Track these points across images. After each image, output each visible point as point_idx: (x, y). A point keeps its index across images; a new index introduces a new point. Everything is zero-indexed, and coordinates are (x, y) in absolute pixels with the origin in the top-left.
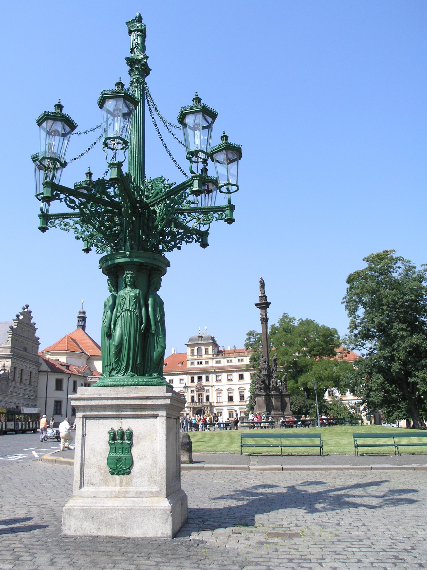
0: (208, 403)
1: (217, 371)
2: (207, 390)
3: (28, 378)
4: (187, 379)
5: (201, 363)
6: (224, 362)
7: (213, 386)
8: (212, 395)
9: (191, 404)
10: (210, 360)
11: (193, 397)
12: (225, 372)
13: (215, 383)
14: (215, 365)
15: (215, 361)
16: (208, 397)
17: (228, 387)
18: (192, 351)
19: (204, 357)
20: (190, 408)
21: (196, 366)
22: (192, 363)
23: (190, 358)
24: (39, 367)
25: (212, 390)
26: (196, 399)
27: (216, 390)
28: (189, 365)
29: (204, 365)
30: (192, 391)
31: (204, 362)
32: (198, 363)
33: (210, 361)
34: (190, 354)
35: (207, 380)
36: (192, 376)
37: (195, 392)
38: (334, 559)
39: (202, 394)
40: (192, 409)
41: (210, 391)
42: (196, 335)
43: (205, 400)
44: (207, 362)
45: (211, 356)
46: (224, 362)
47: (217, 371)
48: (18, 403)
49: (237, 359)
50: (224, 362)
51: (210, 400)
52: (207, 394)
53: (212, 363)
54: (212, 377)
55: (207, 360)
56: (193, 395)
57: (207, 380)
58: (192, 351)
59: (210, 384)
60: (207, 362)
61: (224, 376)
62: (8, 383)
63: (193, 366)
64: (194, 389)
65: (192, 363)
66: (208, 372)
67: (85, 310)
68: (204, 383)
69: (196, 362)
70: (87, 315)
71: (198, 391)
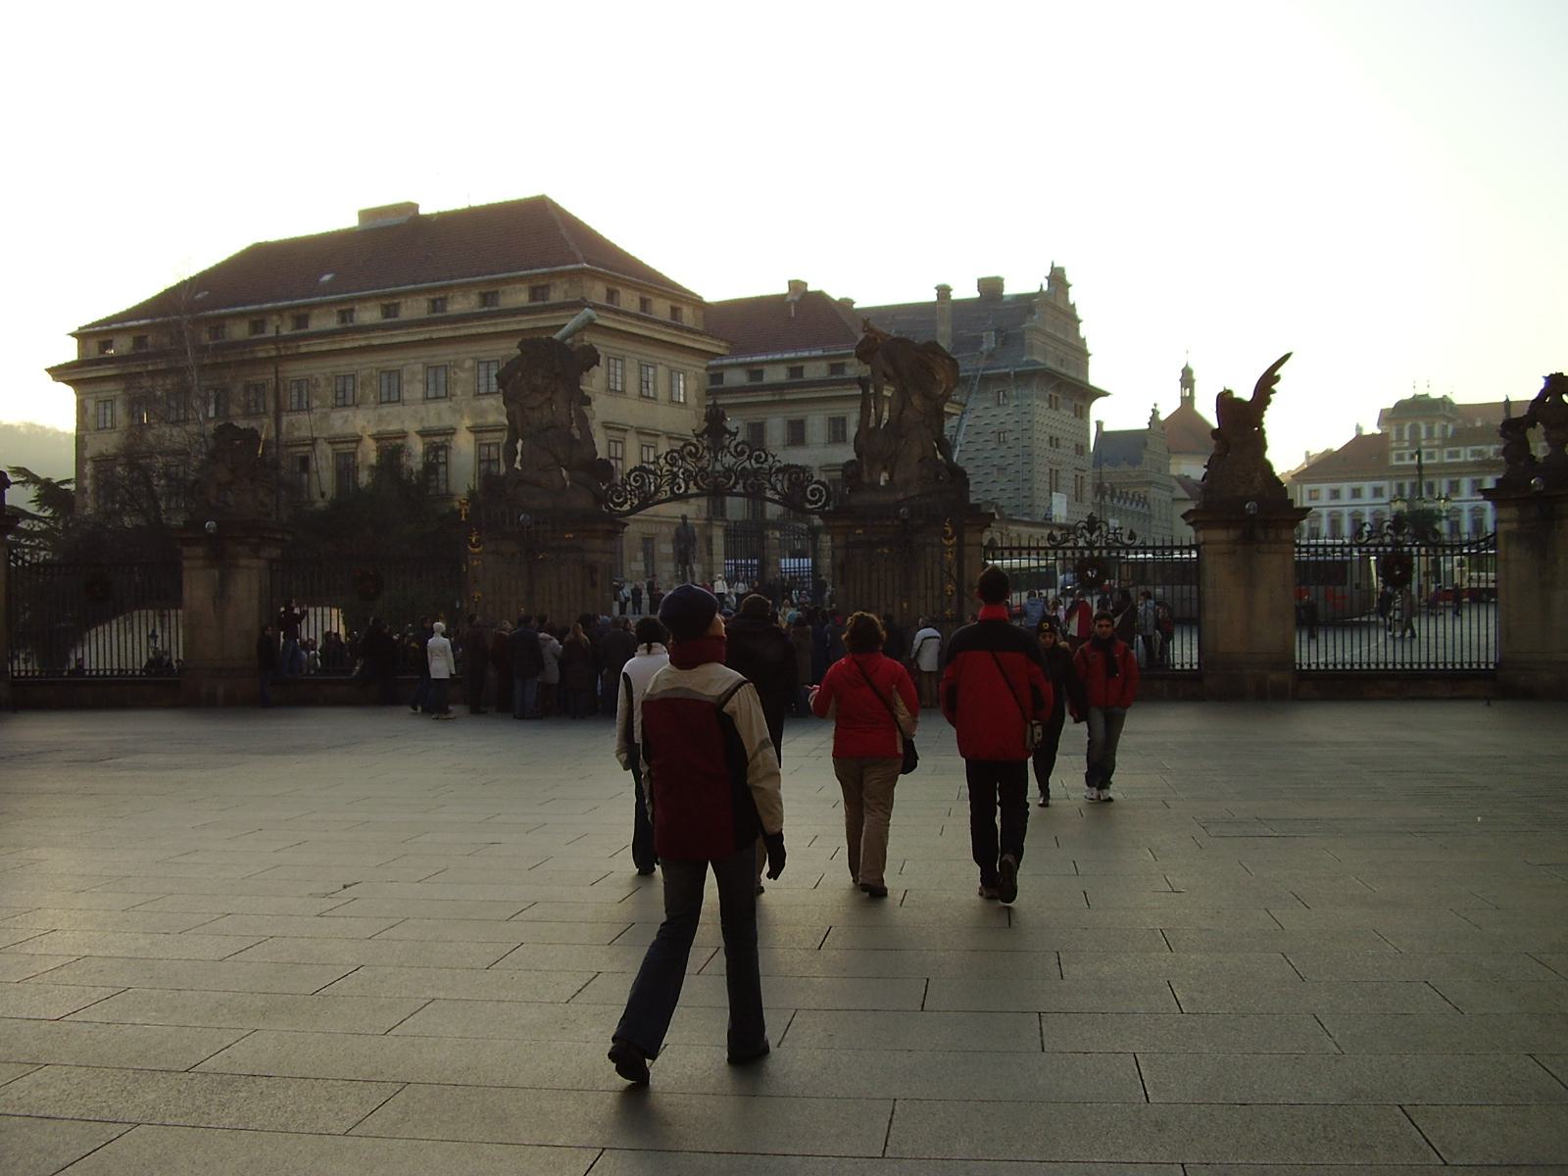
10: (1436, 450)
14: (1447, 460)
15: (1445, 451)
18: (1400, 433)
22: (1400, 457)
23: (1394, 445)
34: (1394, 438)
36: (1400, 481)
45: (1436, 442)
46: (1466, 456)
50: (1466, 456)
53: (1442, 457)
58: (1400, 433)
63: (1400, 463)
65: (1400, 457)
69: (1407, 457)
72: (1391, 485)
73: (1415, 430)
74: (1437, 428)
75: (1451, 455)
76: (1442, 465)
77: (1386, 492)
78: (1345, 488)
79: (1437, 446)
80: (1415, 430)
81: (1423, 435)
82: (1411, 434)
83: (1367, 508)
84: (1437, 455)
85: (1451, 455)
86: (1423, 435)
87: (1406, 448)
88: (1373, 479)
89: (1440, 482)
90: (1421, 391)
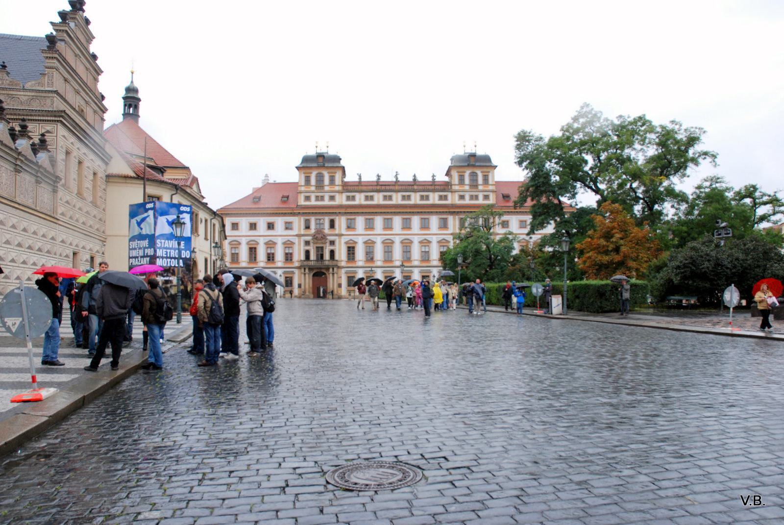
0: (334, 263)
1: (351, 211)
2: (332, 243)
3: (90, 187)
4: (298, 222)
5: (322, 198)
6: (360, 199)
7: (340, 235)
8: (340, 250)
9: (306, 263)
11: (307, 253)
12: (362, 214)
13: (344, 232)
14: (345, 202)
15: (344, 195)
16: (332, 253)
17: (366, 238)
18: (308, 180)
19: (327, 188)
20: (305, 269)
21: (313, 202)
22: (308, 198)
23: (303, 189)
24: (107, 164)
25: (340, 242)
26: (313, 257)
27: (346, 243)
28: (302, 202)
29: (327, 202)
30: (307, 243)
31: (327, 198)
32: (317, 197)
33: (337, 196)
35: (332, 225)
37: (312, 244)
38: (447, 470)
39: (322, 248)
40: (307, 271)
41: (337, 243)
42: (312, 152)
43: (327, 256)
44: (332, 198)
45: (337, 188)
46: (360, 199)
47: (351, 211)
48: (77, 246)
49: (381, 195)
50: (360, 199)
51: (337, 257)
52: (332, 248)
53: (341, 200)
54: (341, 222)
55: (332, 194)
56: (307, 248)
57: (332, 225)
59: (337, 232)
60: (332, 198)
61: (360, 221)
62: (55, 191)
63: (307, 203)
64: (309, 238)
65: (308, 198)
66: (334, 211)
67: (136, 84)
68: (327, 230)
69: (313, 198)
70: (140, 95)
71: (316, 243)
72: (300, 222)
73: (320, 179)
74: (338, 180)
75: (348, 198)
76: (340, 207)
77: (295, 226)
78: (262, 222)
79: (338, 192)
80: (320, 179)
81: (327, 181)
82: (317, 181)
83: (280, 238)
84: (337, 196)
85: (348, 198)
86: (327, 181)
87: (313, 192)
88: (284, 214)
89: (340, 220)
90: (322, 150)
